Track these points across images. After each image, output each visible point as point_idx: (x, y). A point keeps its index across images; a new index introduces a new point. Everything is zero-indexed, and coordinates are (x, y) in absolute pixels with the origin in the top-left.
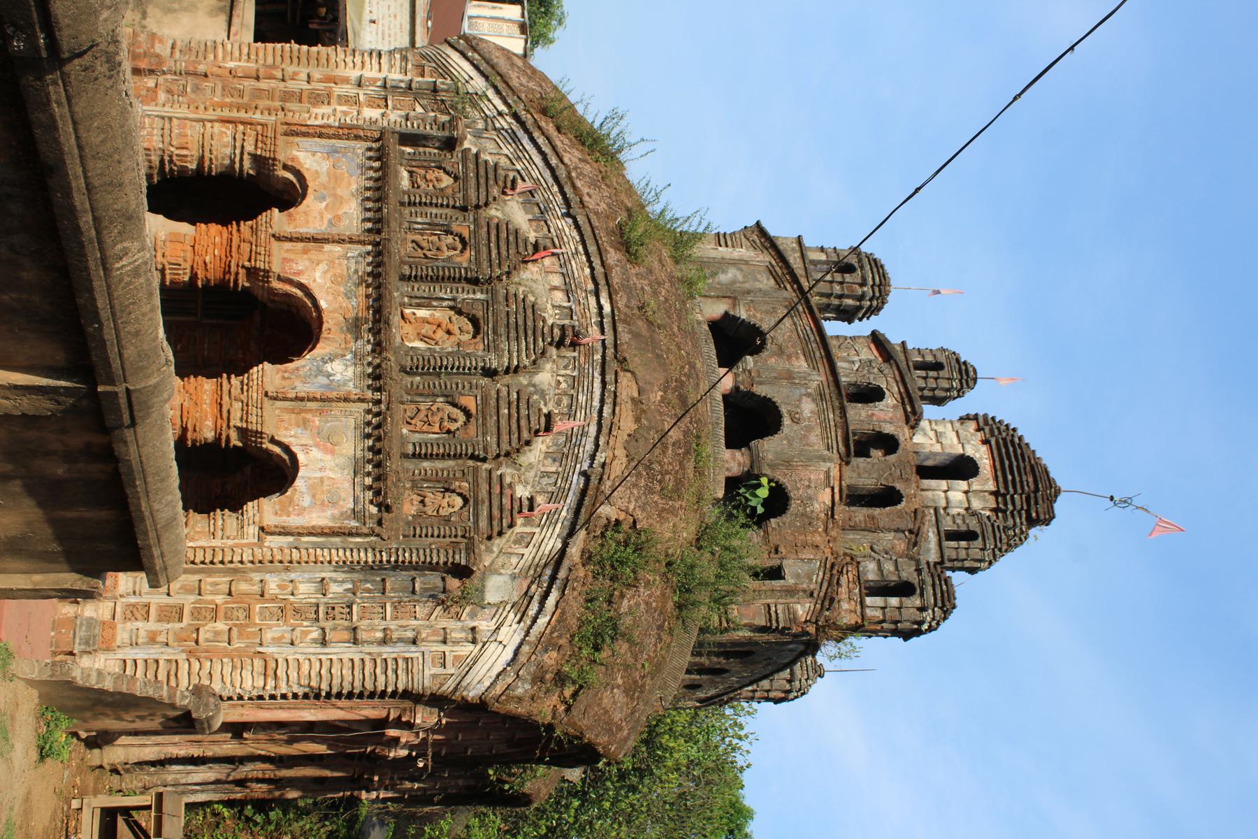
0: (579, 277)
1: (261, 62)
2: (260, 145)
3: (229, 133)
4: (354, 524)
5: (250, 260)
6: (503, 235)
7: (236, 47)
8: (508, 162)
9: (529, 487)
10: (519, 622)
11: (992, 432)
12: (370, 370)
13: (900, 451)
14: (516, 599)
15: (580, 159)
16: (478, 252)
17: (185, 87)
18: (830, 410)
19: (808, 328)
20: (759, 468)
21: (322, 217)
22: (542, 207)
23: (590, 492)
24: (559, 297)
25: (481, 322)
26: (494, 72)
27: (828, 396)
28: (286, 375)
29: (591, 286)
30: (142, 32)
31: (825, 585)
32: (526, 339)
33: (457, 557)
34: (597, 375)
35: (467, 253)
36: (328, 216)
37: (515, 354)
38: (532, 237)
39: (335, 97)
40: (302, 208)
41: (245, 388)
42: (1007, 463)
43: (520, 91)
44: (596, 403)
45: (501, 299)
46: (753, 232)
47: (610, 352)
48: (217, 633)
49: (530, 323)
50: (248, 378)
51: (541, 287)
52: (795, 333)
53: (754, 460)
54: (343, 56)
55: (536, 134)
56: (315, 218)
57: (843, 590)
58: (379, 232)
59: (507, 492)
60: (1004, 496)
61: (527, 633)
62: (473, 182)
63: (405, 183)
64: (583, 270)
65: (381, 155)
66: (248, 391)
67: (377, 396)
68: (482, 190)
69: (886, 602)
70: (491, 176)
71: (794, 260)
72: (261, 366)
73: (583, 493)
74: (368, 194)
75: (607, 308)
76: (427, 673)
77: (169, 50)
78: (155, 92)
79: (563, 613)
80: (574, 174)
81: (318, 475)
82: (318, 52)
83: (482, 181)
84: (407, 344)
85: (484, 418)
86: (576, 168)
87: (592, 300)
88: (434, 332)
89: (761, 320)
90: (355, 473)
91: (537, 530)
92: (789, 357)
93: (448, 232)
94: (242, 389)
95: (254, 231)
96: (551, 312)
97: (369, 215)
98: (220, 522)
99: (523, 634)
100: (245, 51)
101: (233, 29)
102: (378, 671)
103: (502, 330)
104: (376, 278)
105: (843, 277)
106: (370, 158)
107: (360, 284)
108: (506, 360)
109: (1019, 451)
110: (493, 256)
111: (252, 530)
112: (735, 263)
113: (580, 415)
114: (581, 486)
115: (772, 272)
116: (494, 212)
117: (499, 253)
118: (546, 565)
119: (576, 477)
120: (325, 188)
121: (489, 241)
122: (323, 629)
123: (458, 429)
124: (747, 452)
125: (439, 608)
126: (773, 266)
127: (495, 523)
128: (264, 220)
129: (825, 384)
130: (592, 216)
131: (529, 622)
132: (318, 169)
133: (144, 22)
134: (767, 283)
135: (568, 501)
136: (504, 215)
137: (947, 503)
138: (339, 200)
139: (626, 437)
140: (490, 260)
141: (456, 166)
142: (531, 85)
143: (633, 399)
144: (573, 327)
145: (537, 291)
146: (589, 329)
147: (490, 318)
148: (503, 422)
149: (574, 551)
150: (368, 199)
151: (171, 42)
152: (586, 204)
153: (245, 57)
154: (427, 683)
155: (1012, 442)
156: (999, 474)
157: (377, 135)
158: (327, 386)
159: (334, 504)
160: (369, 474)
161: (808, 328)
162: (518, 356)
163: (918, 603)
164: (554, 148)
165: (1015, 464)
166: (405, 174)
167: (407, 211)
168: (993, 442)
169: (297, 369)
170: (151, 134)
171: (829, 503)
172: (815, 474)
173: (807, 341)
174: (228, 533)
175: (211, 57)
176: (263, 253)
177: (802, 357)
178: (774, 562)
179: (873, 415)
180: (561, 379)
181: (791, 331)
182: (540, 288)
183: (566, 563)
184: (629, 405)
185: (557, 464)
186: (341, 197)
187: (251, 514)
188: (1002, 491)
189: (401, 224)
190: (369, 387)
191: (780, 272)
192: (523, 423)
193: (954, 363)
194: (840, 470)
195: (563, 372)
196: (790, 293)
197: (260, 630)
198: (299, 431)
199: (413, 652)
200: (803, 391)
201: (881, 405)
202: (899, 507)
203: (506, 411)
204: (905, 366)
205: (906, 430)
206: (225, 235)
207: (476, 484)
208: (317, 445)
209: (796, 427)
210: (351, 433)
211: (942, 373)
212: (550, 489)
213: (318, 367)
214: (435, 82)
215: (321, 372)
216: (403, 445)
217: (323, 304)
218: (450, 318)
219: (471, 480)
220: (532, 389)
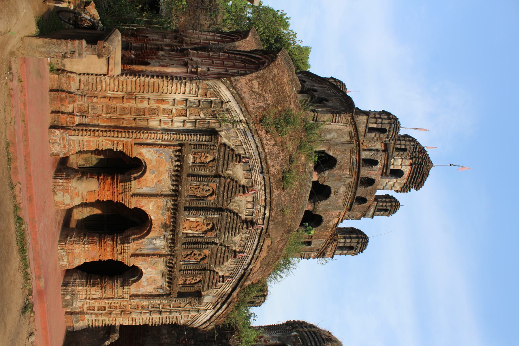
0: (260, 199)
1: (125, 90)
2: (125, 149)
3: (110, 143)
4: (161, 292)
5: (122, 200)
6: (230, 189)
7: (112, 80)
8: (240, 143)
9: (224, 272)
10: (213, 309)
11: (415, 161)
12: (170, 245)
13: (374, 185)
14: (213, 302)
15: (273, 145)
16: (218, 197)
17: (88, 108)
18: (350, 192)
19: (355, 160)
20: (315, 212)
21: (153, 181)
22: (251, 167)
23: (245, 277)
24: (250, 205)
25: (215, 225)
26: (241, 101)
27: (352, 187)
28: (138, 244)
29: (263, 204)
30: (63, 76)
31: (324, 248)
32: (232, 231)
33: (195, 301)
34: (257, 237)
35: (214, 196)
36: (155, 181)
37: (227, 237)
38: (243, 182)
39: (161, 110)
40: (144, 177)
41: (123, 251)
42: (414, 175)
43: (252, 113)
44: (254, 247)
45: (225, 218)
46: (349, 116)
47: (264, 231)
48: (117, 314)
49: (234, 226)
50: (124, 247)
51: (243, 203)
52: (349, 160)
53: (315, 209)
54: (166, 85)
55: (255, 136)
56: (150, 182)
57: (329, 249)
58: (176, 196)
59: (216, 277)
60: (407, 186)
61: (215, 314)
62: (221, 163)
63: (191, 160)
64: (262, 197)
65: (180, 159)
66: (124, 252)
67: (172, 257)
68: (225, 167)
69: (342, 252)
70: (230, 159)
71: (362, 129)
72: (128, 245)
73: (243, 275)
74: (174, 173)
75: (267, 214)
76: (182, 320)
77: (78, 84)
78: (74, 118)
79: (227, 311)
80: (268, 157)
81: (150, 276)
82: (154, 83)
83: (226, 162)
84: (185, 232)
85: (211, 259)
86: (271, 152)
87: (262, 210)
88: (196, 227)
89: (338, 155)
90: (163, 276)
91: (224, 284)
92: (343, 170)
93: (207, 185)
94: (122, 249)
95: (124, 191)
96: (244, 213)
97: (174, 183)
98: (116, 291)
99: (214, 312)
100: (117, 83)
101: (110, 67)
102: (167, 319)
103: (223, 230)
104: (175, 211)
105: (380, 135)
106: (176, 156)
107: (168, 211)
108: (222, 240)
109: (421, 170)
110: (225, 197)
111: (127, 296)
112: (336, 131)
113: (247, 250)
114: (242, 273)
115: (350, 134)
116: (229, 172)
117: (227, 196)
118: (224, 295)
119: (241, 270)
120: (154, 167)
121: (224, 192)
122: (150, 312)
123: (201, 260)
124: (313, 205)
125: (188, 305)
126: (351, 132)
127: (210, 288)
128: (128, 187)
129: (353, 182)
130: (271, 178)
131: (216, 309)
132: (152, 158)
133: (64, 62)
134: (347, 138)
135: (237, 277)
136: (233, 173)
137: (386, 186)
138: (161, 173)
139: (262, 259)
140: (223, 199)
141: (215, 154)
142: (259, 104)
143: (268, 246)
144: (252, 218)
145: (241, 206)
146: (258, 220)
147: (219, 224)
148: (218, 259)
149: (235, 294)
150: (173, 175)
151: (78, 79)
152: (270, 172)
153: (116, 87)
154: (182, 323)
155: (421, 166)
156: (410, 178)
157: (179, 148)
158: (154, 249)
159: (155, 284)
160: (167, 278)
161: (355, 160)
162: (227, 238)
163: (353, 252)
164: (262, 144)
165: (417, 176)
166: (191, 156)
167: (190, 178)
168: (413, 167)
169: (142, 242)
170: (74, 147)
171: (336, 222)
172: (336, 213)
173: (353, 164)
174: (119, 295)
175: (99, 88)
176: (128, 202)
177: (348, 170)
178: (310, 240)
179: (370, 172)
180: (243, 236)
181: (348, 159)
182: (242, 204)
183: (231, 298)
184: (266, 248)
185: (235, 264)
186: (162, 171)
187: (126, 290)
188: (408, 184)
189: (187, 185)
190: (170, 251)
191: (353, 135)
192: (225, 259)
193: (412, 150)
194: (345, 213)
195: (245, 235)
196: (354, 145)
197: (131, 313)
198: (143, 262)
199: (179, 315)
200: (343, 183)
201: (375, 168)
202: (364, 204)
203: (220, 255)
204: (391, 150)
205: (380, 177)
206: (111, 191)
207: (205, 275)
208: (149, 267)
209: (335, 197)
210: (161, 263)
211: (405, 153)
212: (231, 272)
213: (150, 241)
214: (211, 102)
215: (151, 243)
216: (180, 267)
217: (153, 218)
218: (203, 220)
219: (203, 275)
220: (231, 242)
